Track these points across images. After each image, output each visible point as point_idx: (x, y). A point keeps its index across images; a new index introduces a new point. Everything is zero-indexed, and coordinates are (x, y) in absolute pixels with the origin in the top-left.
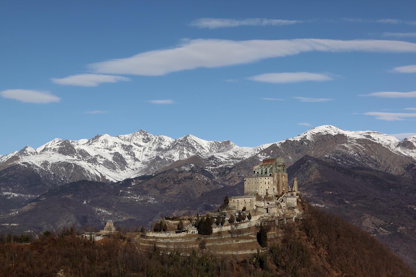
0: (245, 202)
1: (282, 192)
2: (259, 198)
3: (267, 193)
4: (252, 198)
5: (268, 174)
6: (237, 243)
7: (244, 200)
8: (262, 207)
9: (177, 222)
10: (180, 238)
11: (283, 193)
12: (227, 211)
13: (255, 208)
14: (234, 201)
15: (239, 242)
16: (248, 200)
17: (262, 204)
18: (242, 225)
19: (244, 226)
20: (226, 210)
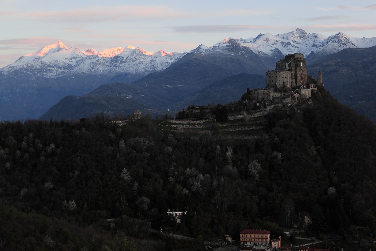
0: (264, 94)
1: (299, 84)
2: (276, 90)
3: (284, 86)
6: (249, 129)
7: (263, 92)
8: (278, 98)
9: (199, 111)
10: (198, 124)
11: (300, 86)
13: (271, 98)
14: (255, 92)
15: (251, 129)
16: (266, 92)
18: (256, 114)
19: (257, 115)
20: (247, 101)
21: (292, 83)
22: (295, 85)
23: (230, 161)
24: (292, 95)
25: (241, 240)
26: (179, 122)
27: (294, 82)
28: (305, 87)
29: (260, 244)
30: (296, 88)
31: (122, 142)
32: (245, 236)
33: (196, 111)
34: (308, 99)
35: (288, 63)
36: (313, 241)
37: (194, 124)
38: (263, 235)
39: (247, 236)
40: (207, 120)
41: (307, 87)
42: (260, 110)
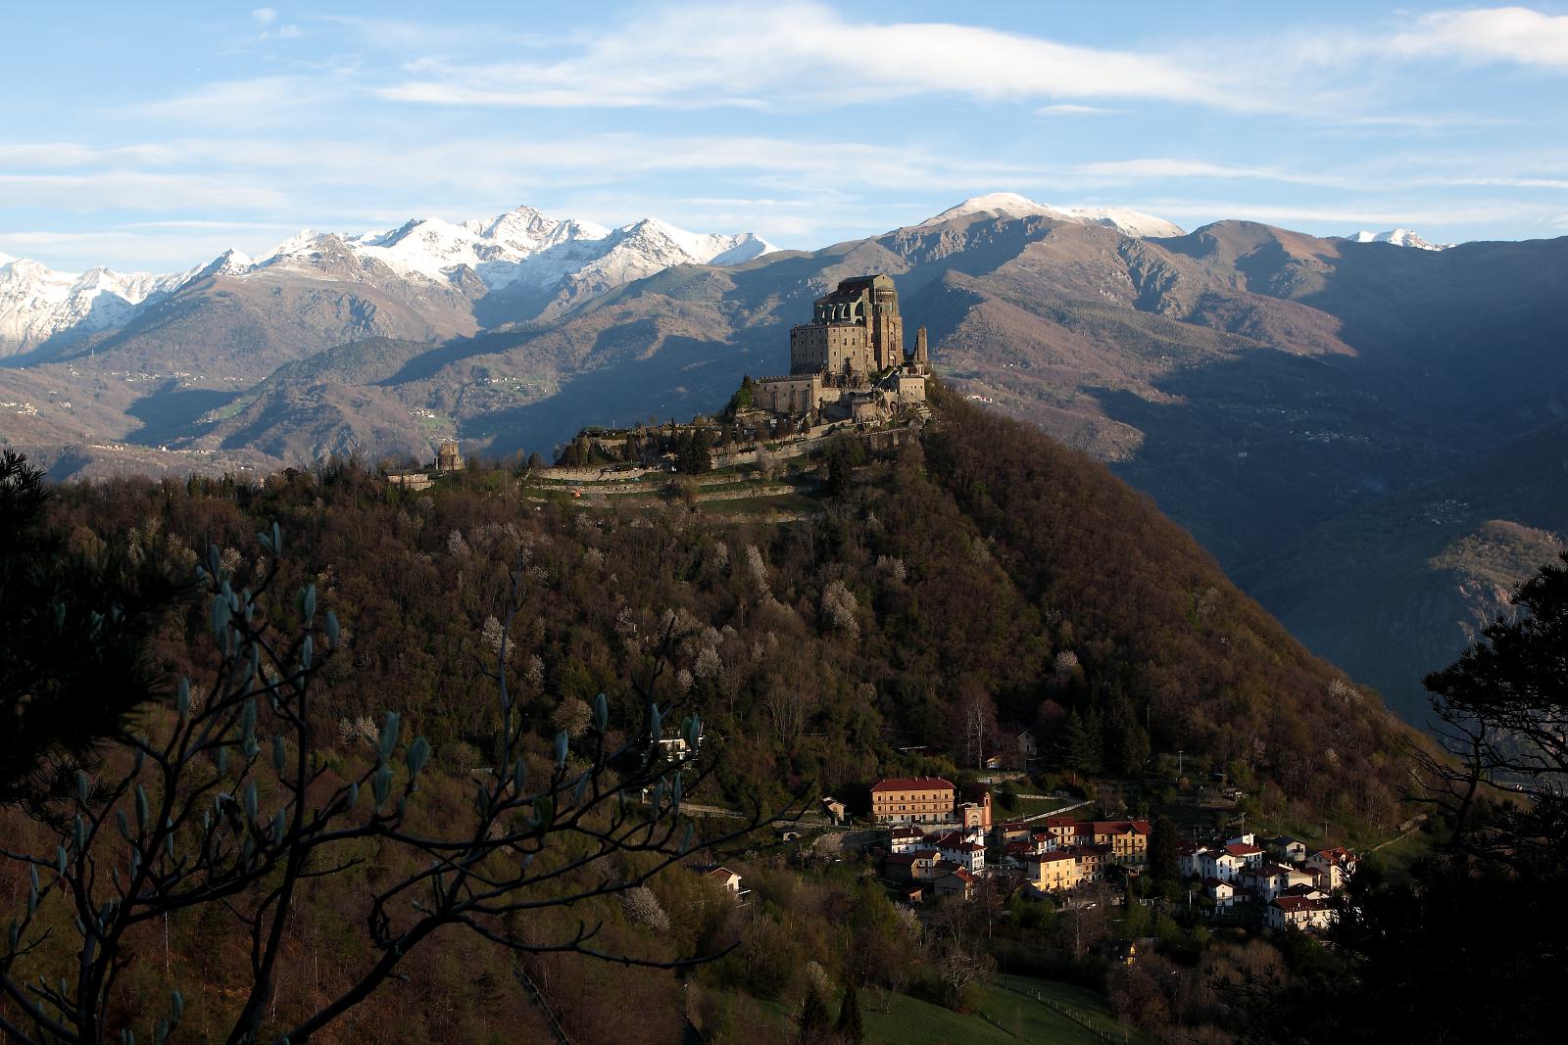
3: (848, 368)
5: (854, 319)
6: (774, 494)
15: (779, 493)
16: (800, 385)
23: (763, 586)
25: (875, 808)
26: (571, 476)
27: (872, 356)
29: (930, 817)
30: (884, 379)
31: (456, 537)
32: (888, 799)
36: (1063, 804)
37: (616, 482)
38: (936, 792)
39: (891, 798)
41: (909, 372)
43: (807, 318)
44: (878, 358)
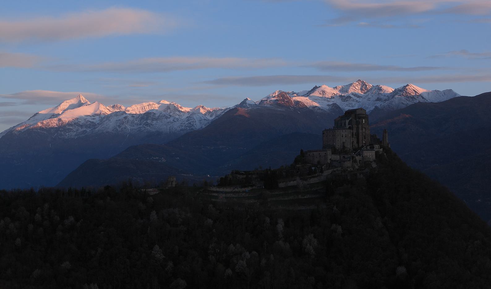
0: (320, 156)
2: (335, 152)
3: (344, 147)
4: (326, 151)
6: (303, 198)
7: (319, 154)
8: (337, 161)
9: (245, 176)
10: (243, 192)
11: (363, 146)
12: (301, 165)
13: (329, 161)
15: (305, 197)
17: (337, 157)
19: (313, 181)
20: (301, 164)
21: (353, 144)
22: (356, 145)
24: (353, 157)
26: (221, 190)
27: (355, 142)
28: (368, 148)
30: (358, 150)
31: (154, 213)
33: (241, 177)
34: (371, 162)
35: (348, 121)
37: (239, 192)
40: (254, 187)
41: (370, 148)
42: (316, 175)
43: (331, 125)
44: (358, 142)
